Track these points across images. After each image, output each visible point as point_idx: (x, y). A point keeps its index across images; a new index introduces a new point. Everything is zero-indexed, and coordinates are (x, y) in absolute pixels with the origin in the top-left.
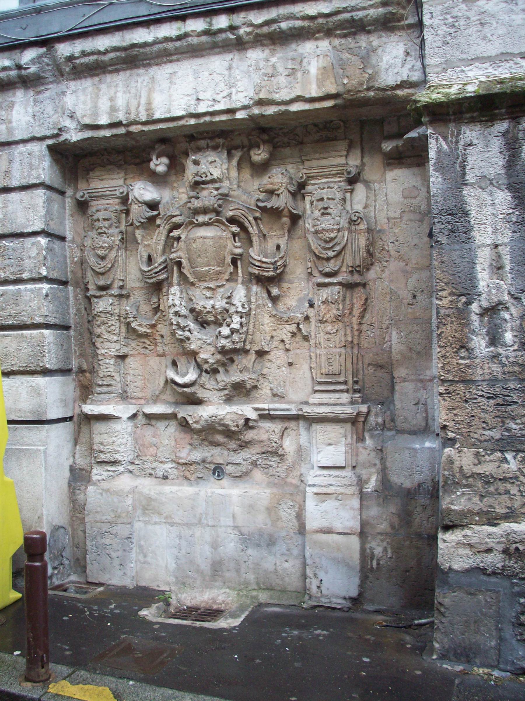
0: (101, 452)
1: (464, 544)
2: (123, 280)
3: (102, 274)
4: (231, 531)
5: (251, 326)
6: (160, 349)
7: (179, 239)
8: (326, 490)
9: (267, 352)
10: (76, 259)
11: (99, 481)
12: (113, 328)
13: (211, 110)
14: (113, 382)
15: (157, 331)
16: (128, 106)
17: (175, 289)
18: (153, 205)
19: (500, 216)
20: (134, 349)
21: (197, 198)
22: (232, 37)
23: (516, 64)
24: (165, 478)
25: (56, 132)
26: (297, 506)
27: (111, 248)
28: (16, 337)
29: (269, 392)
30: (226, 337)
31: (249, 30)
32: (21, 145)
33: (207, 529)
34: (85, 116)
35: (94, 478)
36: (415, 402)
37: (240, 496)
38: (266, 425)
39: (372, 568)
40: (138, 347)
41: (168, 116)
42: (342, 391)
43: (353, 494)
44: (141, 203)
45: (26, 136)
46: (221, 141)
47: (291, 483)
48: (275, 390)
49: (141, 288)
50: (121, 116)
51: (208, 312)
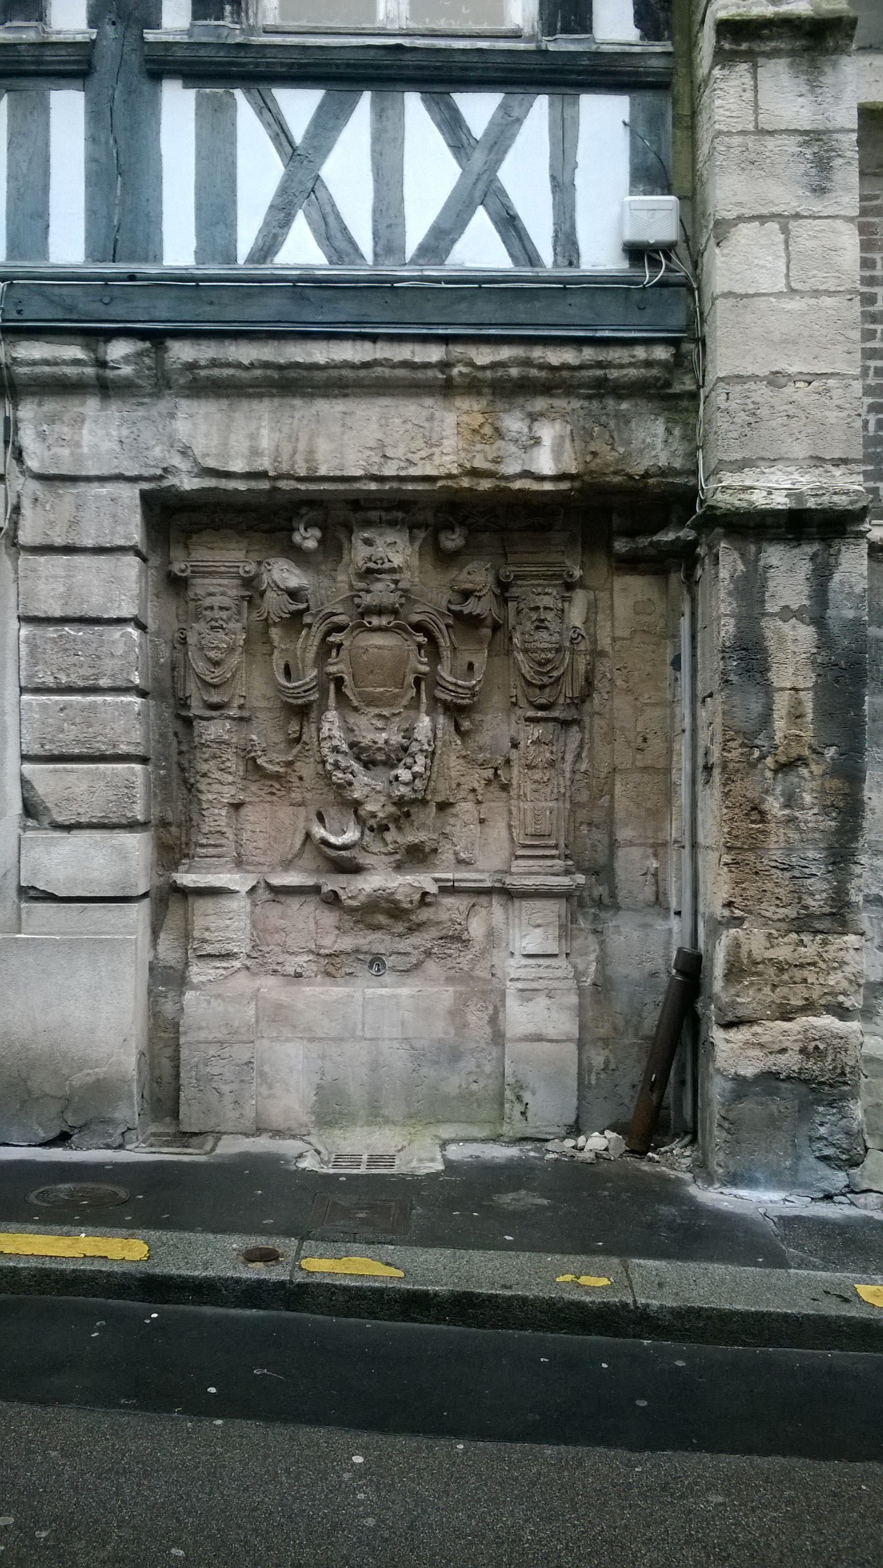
0: (205, 941)
1: (753, 1044)
2: (244, 697)
3: (215, 686)
4: (398, 1046)
5: (435, 769)
6: (296, 796)
7: (339, 646)
8: (535, 985)
9: (451, 805)
10: (162, 660)
11: (203, 983)
12: (228, 764)
13: (403, 473)
14: (224, 841)
15: (294, 771)
16: (277, 450)
17: (332, 715)
18: (294, 594)
19: (804, 656)
20: (254, 794)
21: (368, 591)
22: (440, 376)
23: (826, 471)
24: (298, 975)
25: (159, 472)
26: (491, 1008)
27: (231, 650)
28: (87, 772)
29: (452, 857)
30: (406, 784)
31: (464, 370)
32: (96, 484)
33: (365, 1044)
34: (208, 455)
35: (195, 979)
36: (643, 872)
37: (413, 997)
38: (448, 901)
39: (590, 1084)
40: (262, 793)
41: (338, 473)
42: (552, 857)
43: (569, 990)
44: (282, 590)
45: (105, 471)
46: (400, 515)
47: (479, 978)
48: (462, 854)
49: (270, 710)
50: (265, 464)
51: (379, 749)
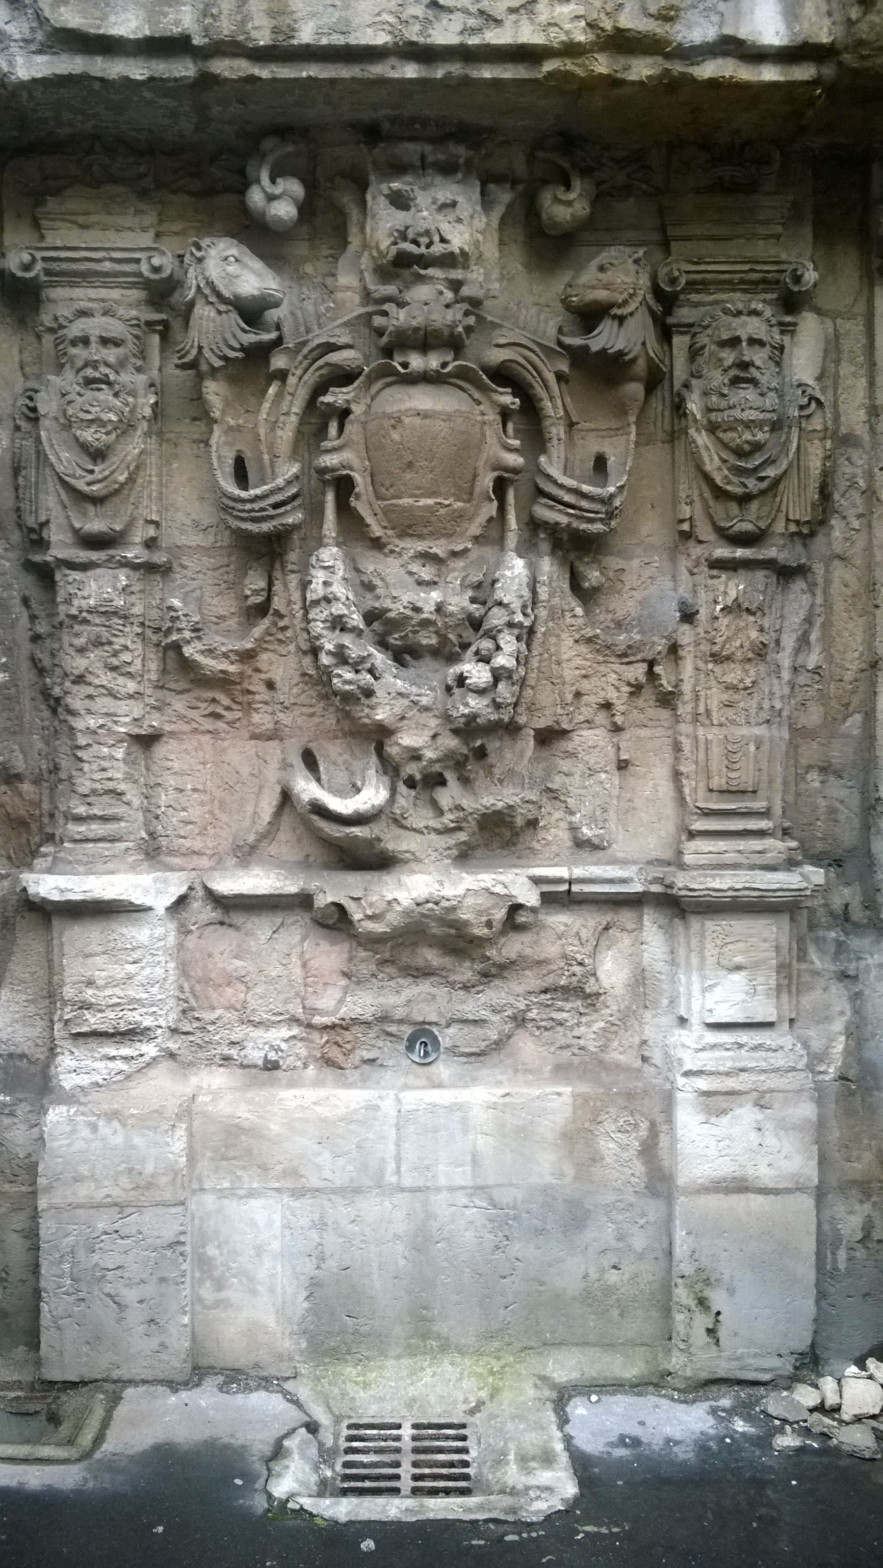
0: (86, 1006)
2: (157, 524)
3: (97, 501)
4: (465, 1201)
5: (534, 662)
7: (344, 414)
8: (731, 1083)
9: (563, 734)
12: (126, 657)
15: (258, 670)
17: (330, 554)
20: (181, 717)
21: (401, 305)
26: (644, 1125)
27: (125, 427)
29: (564, 835)
30: (481, 692)
35: (68, 1082)
37: (494, 1106)
39: (836, 1269)
41: (338, 40)
42: (761, 834)
43: (799, 1091)
46: (461, 152)
47: (618, 1066)
48: (585, 830)
51: (426, 623)
